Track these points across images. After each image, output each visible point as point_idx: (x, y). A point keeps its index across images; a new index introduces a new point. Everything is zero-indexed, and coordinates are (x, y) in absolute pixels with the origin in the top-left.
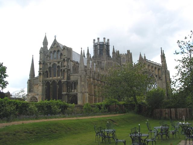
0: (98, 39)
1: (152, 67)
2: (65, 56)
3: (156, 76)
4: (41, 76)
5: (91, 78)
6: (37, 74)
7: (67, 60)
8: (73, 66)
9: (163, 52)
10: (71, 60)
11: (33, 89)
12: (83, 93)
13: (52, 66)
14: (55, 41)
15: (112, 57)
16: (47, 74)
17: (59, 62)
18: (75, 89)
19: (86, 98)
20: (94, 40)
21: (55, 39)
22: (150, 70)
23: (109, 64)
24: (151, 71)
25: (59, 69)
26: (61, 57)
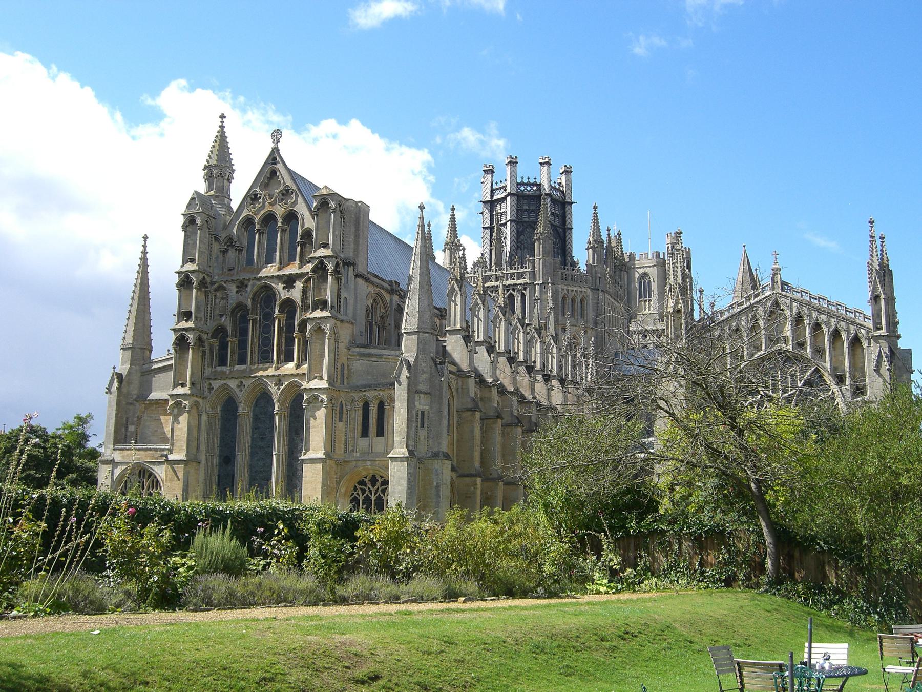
0: (513, 162)
1: (817, 327)
2: (325, 246)
3: (840, 380)
7: (336, 271)
8: (370, 303)
10: (361, 269)
12: (420, 461)
13: (253, 300)
14: (274, 157)
16: (223, 346)
19: (438, 487)
23: (569, 301)
25: (291, 316)
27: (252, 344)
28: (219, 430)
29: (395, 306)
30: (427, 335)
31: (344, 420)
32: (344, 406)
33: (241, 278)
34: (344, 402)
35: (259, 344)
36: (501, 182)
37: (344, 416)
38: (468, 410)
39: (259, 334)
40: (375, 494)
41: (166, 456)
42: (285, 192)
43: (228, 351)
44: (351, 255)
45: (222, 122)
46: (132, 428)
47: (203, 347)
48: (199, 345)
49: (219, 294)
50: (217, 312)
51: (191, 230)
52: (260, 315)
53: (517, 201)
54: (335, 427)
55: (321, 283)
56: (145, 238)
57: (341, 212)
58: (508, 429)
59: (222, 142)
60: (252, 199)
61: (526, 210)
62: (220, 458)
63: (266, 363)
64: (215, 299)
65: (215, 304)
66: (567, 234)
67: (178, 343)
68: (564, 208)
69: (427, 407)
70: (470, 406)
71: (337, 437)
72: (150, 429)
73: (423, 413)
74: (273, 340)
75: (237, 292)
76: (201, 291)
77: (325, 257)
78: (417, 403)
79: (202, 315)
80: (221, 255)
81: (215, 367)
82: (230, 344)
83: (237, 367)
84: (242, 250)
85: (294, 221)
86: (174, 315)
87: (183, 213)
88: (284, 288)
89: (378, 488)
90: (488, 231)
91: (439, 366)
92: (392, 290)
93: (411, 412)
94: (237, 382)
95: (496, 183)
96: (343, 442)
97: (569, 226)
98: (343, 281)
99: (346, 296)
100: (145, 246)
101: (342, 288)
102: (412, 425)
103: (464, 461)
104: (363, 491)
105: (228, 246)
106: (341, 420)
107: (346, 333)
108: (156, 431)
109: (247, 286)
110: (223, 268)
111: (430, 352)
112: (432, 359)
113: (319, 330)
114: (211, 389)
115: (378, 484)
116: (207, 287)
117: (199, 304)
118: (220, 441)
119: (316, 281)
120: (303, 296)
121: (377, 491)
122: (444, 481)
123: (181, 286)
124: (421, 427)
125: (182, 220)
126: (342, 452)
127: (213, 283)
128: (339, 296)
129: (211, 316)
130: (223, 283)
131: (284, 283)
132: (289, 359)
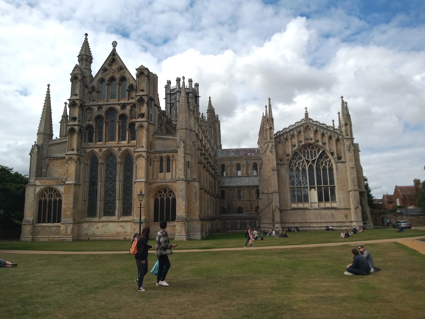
1: (323, 135)
2: (143, 91)
3: (332, 154)
6: (56, 134)
11: (47, 169)
18: (168, 171)
19: (196, 193)
20: (169, 82)
21: (114, 50)
24: (320, 143)
26: (129, 95)
31: (152, 165)
32: (152, 159)
34: (152, 158)
36: (174, 87)
37: (152, 164)
39: (109, 129)
40: (166, 196)
41: (64, 182)
42: (120, 68)
45: (86, 37)
46: (44, 170)
47: (82, 133)
49: (88, 111)
52: (109, 121)
54: (148, 168)
56: (49, 85)
59: (86, 45)
60: (103, 70)
67: (70, 131)
69: (190, 160)
71: (149, 172)
72: (54, 171)
73: (188, 162)
75: (98, 110)
77: (143, 95)
79: (81, 119)
80: (89, 94)
81: (87, 143)
82: (94, 132)
83: (98, 143)
84: (99, 92)
85: (124, 82)
86: (59, 122)
87: (71, 73)
88: (121, 109)
89: (167, 194)
95: (172, 87)
98: (150, 106)
99: (151, 113)
100: (48, 89)
104: (160, 195)
105: (92, 90)
106: (150, 165)
107: (152, 128)
109: (102, 108)
110: (90, 100)
113: (141, 126)
114: (85, 152)
115: (167, 192)
116: (83, 108)
118: (90, 175)
119: (139, 106)
120: (130, 113)
121: (167, 195)
125: (70, 77)
126: (152, 179)
128: (148, 113)
129: (84, 121)
130: (90, 106)
131: (121, 107)
132: (124, 139)
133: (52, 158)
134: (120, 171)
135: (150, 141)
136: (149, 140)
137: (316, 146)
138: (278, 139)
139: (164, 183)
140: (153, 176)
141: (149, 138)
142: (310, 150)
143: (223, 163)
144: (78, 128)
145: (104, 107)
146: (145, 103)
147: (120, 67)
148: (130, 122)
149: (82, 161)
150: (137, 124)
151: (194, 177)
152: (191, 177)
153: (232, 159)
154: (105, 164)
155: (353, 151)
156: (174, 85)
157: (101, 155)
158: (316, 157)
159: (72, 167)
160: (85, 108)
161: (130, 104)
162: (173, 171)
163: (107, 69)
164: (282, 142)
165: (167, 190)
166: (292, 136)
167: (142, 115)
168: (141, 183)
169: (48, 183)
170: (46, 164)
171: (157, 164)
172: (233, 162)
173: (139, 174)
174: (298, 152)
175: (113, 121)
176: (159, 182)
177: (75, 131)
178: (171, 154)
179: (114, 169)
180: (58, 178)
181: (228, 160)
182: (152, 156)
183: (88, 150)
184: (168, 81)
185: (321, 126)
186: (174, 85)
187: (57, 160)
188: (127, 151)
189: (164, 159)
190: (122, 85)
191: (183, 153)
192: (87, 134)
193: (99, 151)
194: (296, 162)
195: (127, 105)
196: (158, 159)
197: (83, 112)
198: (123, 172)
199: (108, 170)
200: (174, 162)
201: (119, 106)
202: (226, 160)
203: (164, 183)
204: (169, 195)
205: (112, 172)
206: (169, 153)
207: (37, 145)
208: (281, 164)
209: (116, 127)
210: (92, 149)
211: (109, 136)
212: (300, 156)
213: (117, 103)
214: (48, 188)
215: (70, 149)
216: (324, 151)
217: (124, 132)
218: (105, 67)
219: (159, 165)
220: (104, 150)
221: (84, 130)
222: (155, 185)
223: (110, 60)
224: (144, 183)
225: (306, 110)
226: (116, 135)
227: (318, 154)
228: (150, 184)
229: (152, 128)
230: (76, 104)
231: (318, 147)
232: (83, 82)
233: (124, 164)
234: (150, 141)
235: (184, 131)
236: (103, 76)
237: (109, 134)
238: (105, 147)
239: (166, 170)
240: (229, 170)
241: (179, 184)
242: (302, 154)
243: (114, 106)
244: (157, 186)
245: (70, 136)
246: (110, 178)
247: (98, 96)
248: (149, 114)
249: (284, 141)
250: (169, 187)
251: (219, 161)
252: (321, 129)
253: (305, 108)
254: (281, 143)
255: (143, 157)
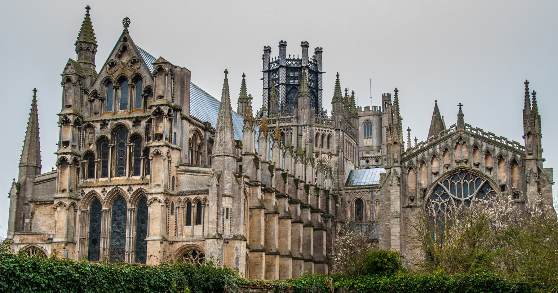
0: (283, 45)
2: (161, 97)
4: (67, 171)
5: (257, 186)
7: (169, 115)
8: (191, 136)
9: (534, 98)
10: (185, 113)
11: (32, 219)
12: (226, 241)
14: (125, 38)
15: (329, 115)
16: (92, 166)
17: (137, 122)
18: (199, 222)
19: (237, 258)
20: (268, 50)
22: (477, 165)
25: (138, 146)
27: (111, 164)
28: (89, 221)
29: (207, 138)
30: (230, 157)
31: (175, 214)
32: (175, 205)
33: (104, 119)
34: (174, 202)
35: (116, 163)
36: (276, 58)
37: (175, 211)
38: (257, 208)
39: (117, 157)
41: (52, 239)
42: (133, 61)
43: (94, 168)
44: (179, 104)
46: (27, 221)
47: (78, 165)
48: (75, 164)
49: (88, 130)
50: (87, 142)
51: (68, 86)
52: (117, 144)
53: (286, 71)
54: (169, 219)
55: (159, 123)
57: (172, 75)
58: (282, 220)
60: (110, 65)
61: (292, 77)
62: (90, 240)
63: (122, 176)
64: (86, 133)
65: (85, 137)
66: (319, 93)
67: (60, 162)
68: (317, 76)
70: (258, 204)
71: (170, 225)
72: (41, 221)
73: (227, 209)
74: (126, 161)
75: (101, 129)
76: (76, 127)
77: (161, 105)
78: (223, 203)
79: (76, 144)
80: (89, 104)
82: (96, 163)
83: (101, 179)
84: (104, 100)
85: (140, 82)
86: (57, 144)
88: (133, 126)
89: (197, 259)
90: (267, 91)
91: (238, 178)
92: (206, 127)
93: (220, 208)
94: (101, 189)
95: (273, 59)
96: (174, 229)
97: (320, 88)
101: (173, 126)
102: (220, 218)
103: (254, 241)
105: (94, 97)
106: (172, 214)
108: (45, 222)
109: (107, 124)
110: (91, 113)
111: (232, 169)
112: (234, 173)
113: (158, 154)
114: (83, 193)
115: (197, 256)
116: (80, 125)
117: (75, 137)
118: (90, 228)
119: (155, 121)
120: (146, 131)
122: (242, 254)
123: (62, 124)
124: (226, 218)
126: (174, 235)
127: (84, 122)
128: (171, 132)
129: (82, 145)
130: (91, 123)
131: (134, 122)
132: (137, 173)
133: (38, 203)
134: (131, 223)
135: (173, 176)
136: (171, 174)
137: (474, 173)
138: (408, 161)
139: (191, 243)
140: (176, 230)
141: (170, 171)
142: (464, 181)
143: (358, 196)
144: (71, 158)
145: (110, 123)
146: (165, 117)
147: (133, 60)
148: (145, 146)
149: (78, 207)
150: (152, 150)
151: (236, 233)
152: (231, 232)
153: (374, 189)
154: (111, 212)
155: (536, 184)
156: (275, 54)
157: (104, 198)
158: (474, 194)
159: (62, 216)
160: (83, 126)
161: (145, 117)
162: (204, 222)
163: (114, 64)
164: (414, 167)
165: (198, 252)
166: (432, 156)
167: (159, 137)
168: (155, 242)
169: (31, 239)
170: (31, 212)
171: (182, 212)
172: (376, 194)
173: (153, 228)
174: (442, 185)
175: (122, 145)
176: (185, 240)
177: (67, 162)
178: (202, 197)
179: (123, 220)
180: (44, 233)
181: (368, 190)
182: (175, 199)
183: (87, 191)
184: (265, 47)
185: (485, 138)
186: (275, 54)
187: (46, 205)
188: (139, 191)
189: (193, 204)
190: (137, 87)
191: (216, 195)
192: (87, 165)
193: (102, 192)
194: (438, 203)
195: (143, 119)
196: (182, 204)
197: (80, 133)
198: (134, 224)
199: (114, 220)
200: (206, 209)
201: (130, 120)
202: (363, 190)
203: (191, 243)
204: (199, 261)
205: (120, 224)
206: (199, 194)
207: (16, 183)
208: (411, 207)
209: (126, 154)
210: (91, 189)
211: (116, 168)
212: (445, 191)
213: (127, 116)
214: (30, 247)
215: (60, 188)
216: (487, 183)
217: (137, 162)
218: (112, 60)
219: (185, 213)
220: (109, 190)
221: (82, 159)
222: (178, 246)
223: (119, 49)
224: (159, 242)
225: (460, 108)
226: (126, 167)
227: (476, 189)
228: (171, 243)
229: (175, 156)
230: (68, 120)
231: (478, 175)
232: (80, 85)
233: (137, 211)
234: (172, 175)
235: (221, 158)
236: (109, 75)
237: (116, 166)
238: (110, 186)
239: (195, 221)
240: (370, 210)
241: (209, 244)
242: (447, 187)
243: (123, 121)
244: (181, 246)
245: (61, 170)
246: (118, 233)
247: (101, 105)
248: (172, 133)
249: (418, 164)
250: (198, 248)
251: (351, 194)
252: (483, 143)
253: (458, 106)
254: (412, 168)
255: (159, 202)
